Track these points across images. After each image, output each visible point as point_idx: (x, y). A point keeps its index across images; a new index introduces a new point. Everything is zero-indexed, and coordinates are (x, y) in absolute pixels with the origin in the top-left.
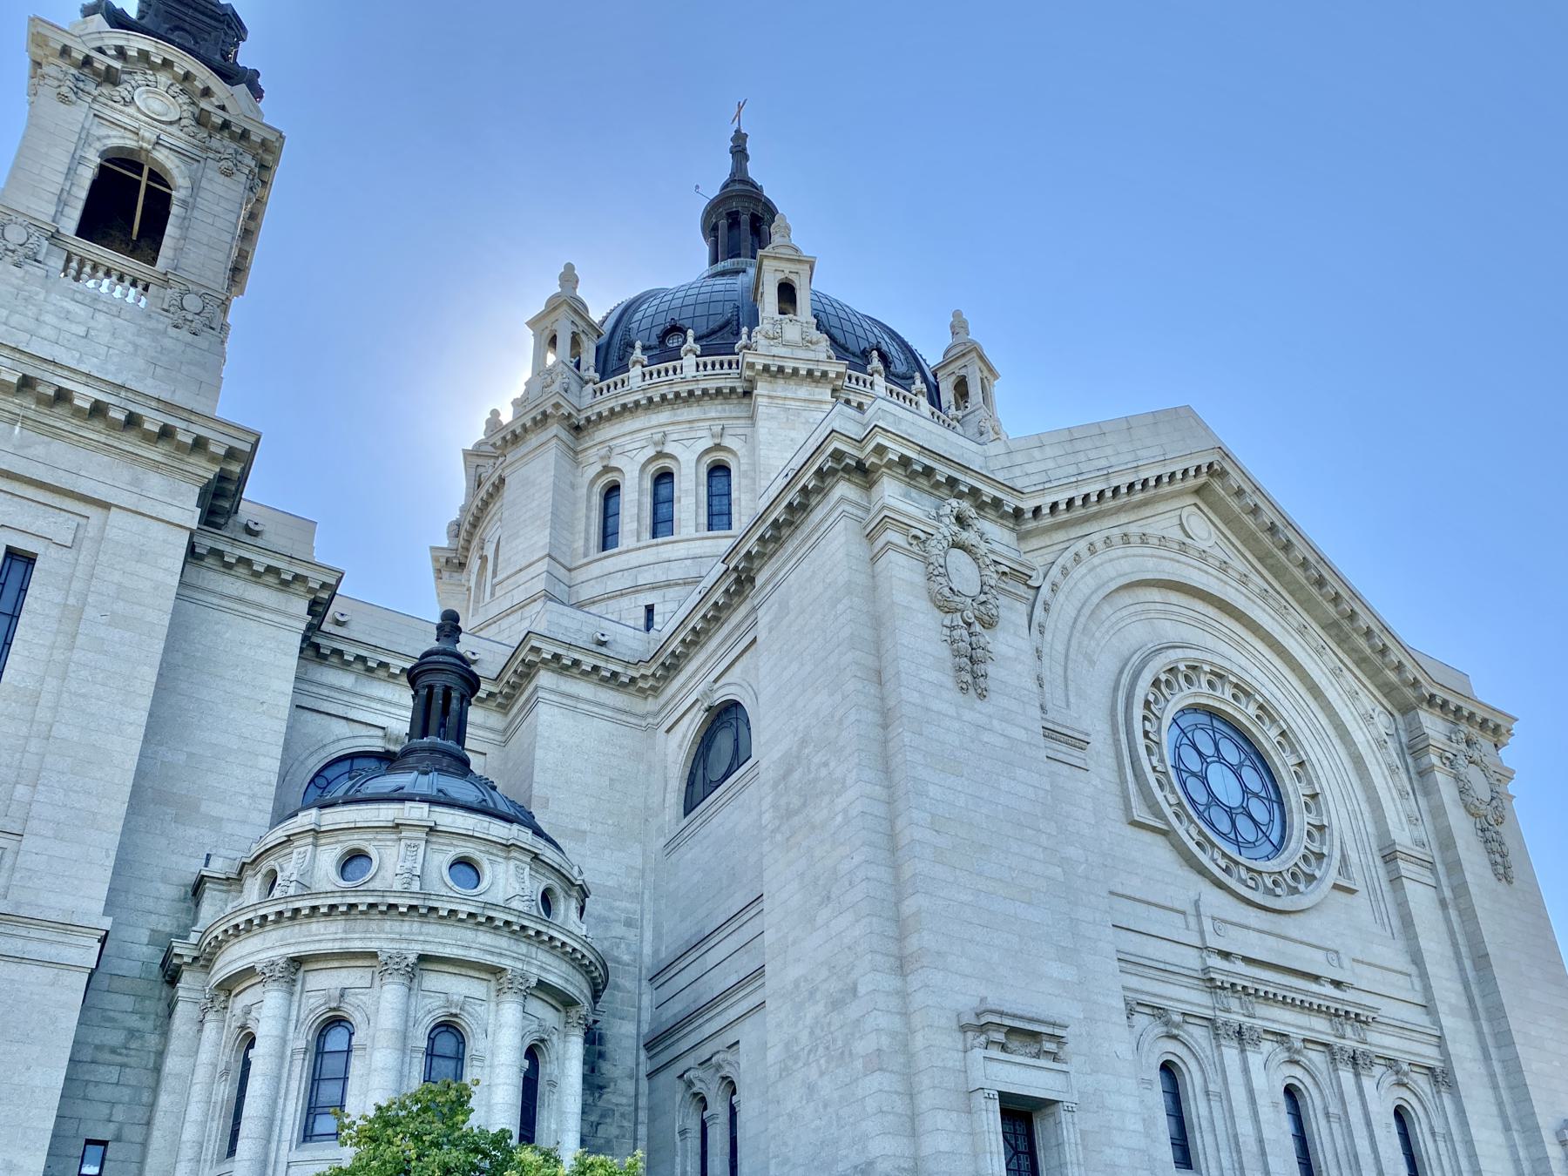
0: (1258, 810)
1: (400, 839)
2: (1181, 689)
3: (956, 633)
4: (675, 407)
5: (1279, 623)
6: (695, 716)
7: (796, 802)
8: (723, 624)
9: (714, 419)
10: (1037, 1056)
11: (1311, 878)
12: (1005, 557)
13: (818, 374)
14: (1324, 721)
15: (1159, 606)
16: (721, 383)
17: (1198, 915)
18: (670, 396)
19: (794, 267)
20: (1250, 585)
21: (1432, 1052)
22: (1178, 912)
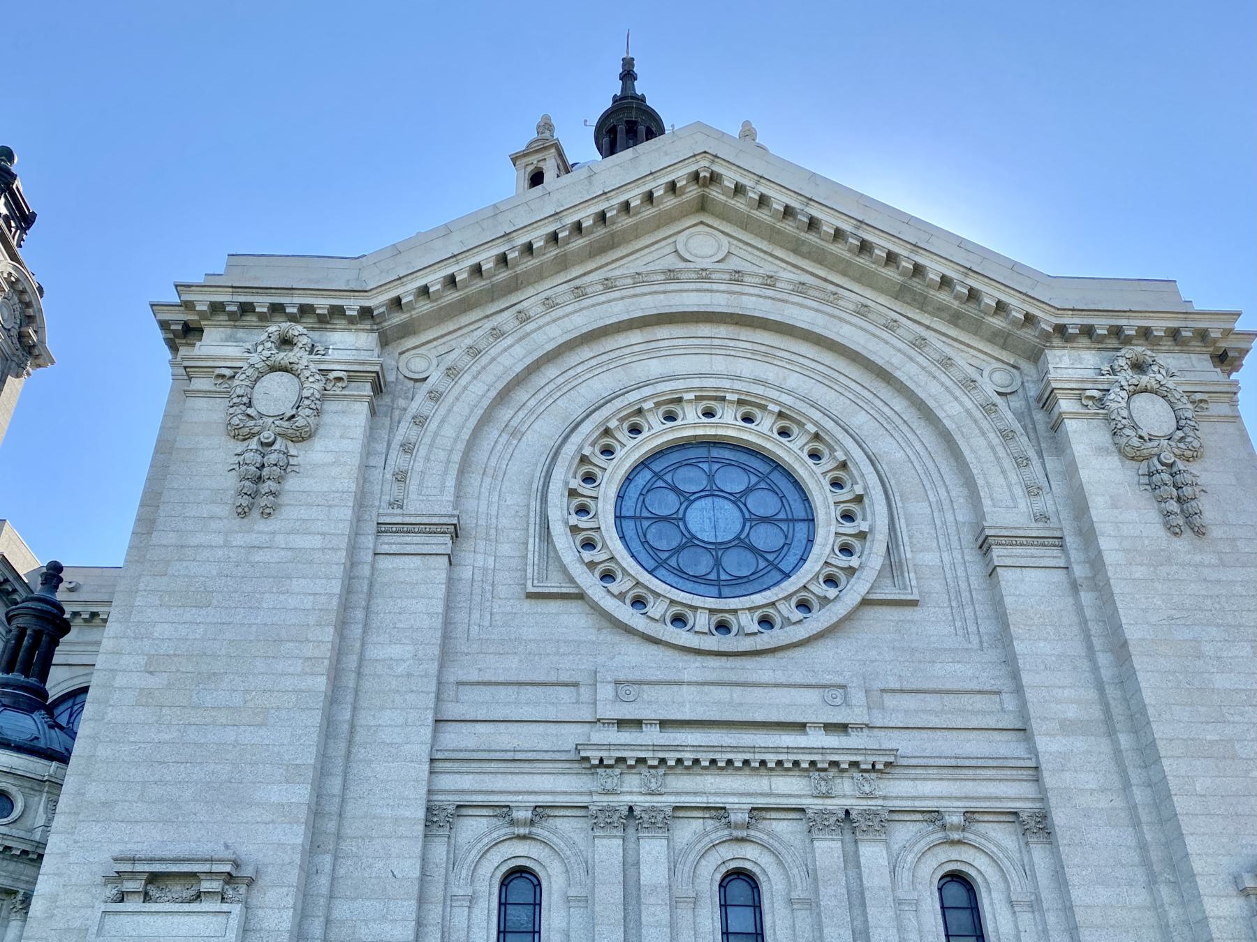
15: (636, 348)
22: (566, 685)
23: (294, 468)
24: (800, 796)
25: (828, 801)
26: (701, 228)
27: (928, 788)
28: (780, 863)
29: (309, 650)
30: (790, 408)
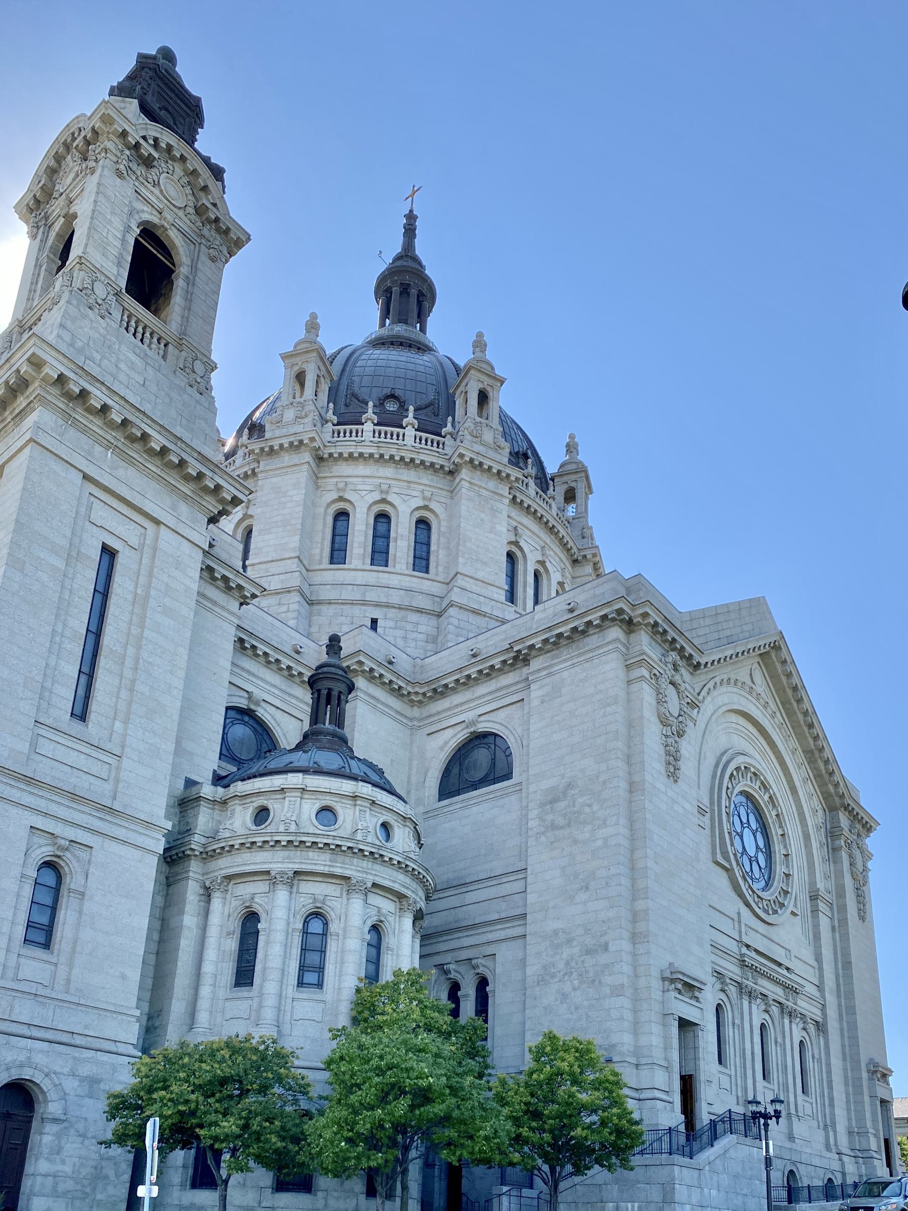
1: (355, 805)
4: (399, 466)
6: (459, 732)
7: (560, 821)
8: (491, 679)
9: (425, 485)
11: (782, 905)
13: (504, 475)
16: (435, 460)
17: (740, 922)
18: (397, 458)
19: (491, 382)
21: (819, 1012)
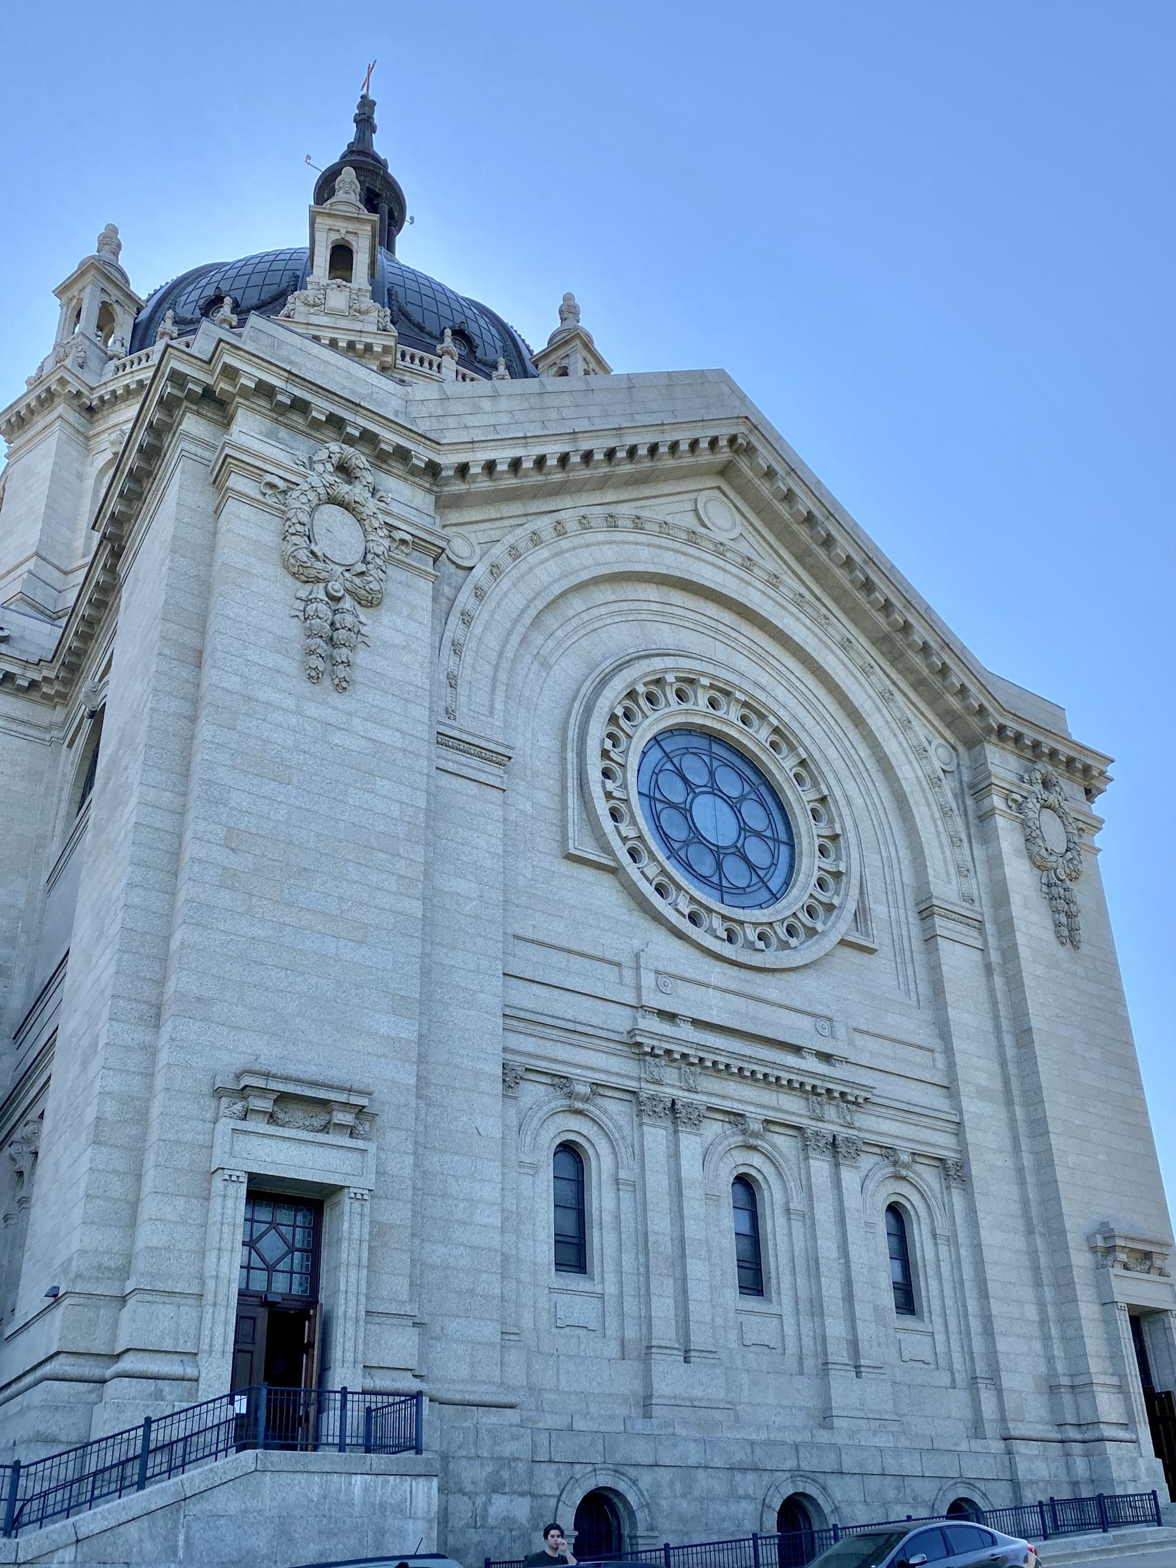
0: (757, 852)
2: (668, 704)
3: (311, 609)
5: (816, 635)
10: (325, 1129)
11: (812, 932)
12: (405, 521)
14: (864, 752)
15: (654, 607)
20: (781, 588)
22: (610, 963)
23: (365, 639)
24: (800, 1116)
25: (821, 1124)
26: (717, 493)
27: (887, 1126)
28: (780, 1174)
29: (401, 867)
30: (786, 725)
